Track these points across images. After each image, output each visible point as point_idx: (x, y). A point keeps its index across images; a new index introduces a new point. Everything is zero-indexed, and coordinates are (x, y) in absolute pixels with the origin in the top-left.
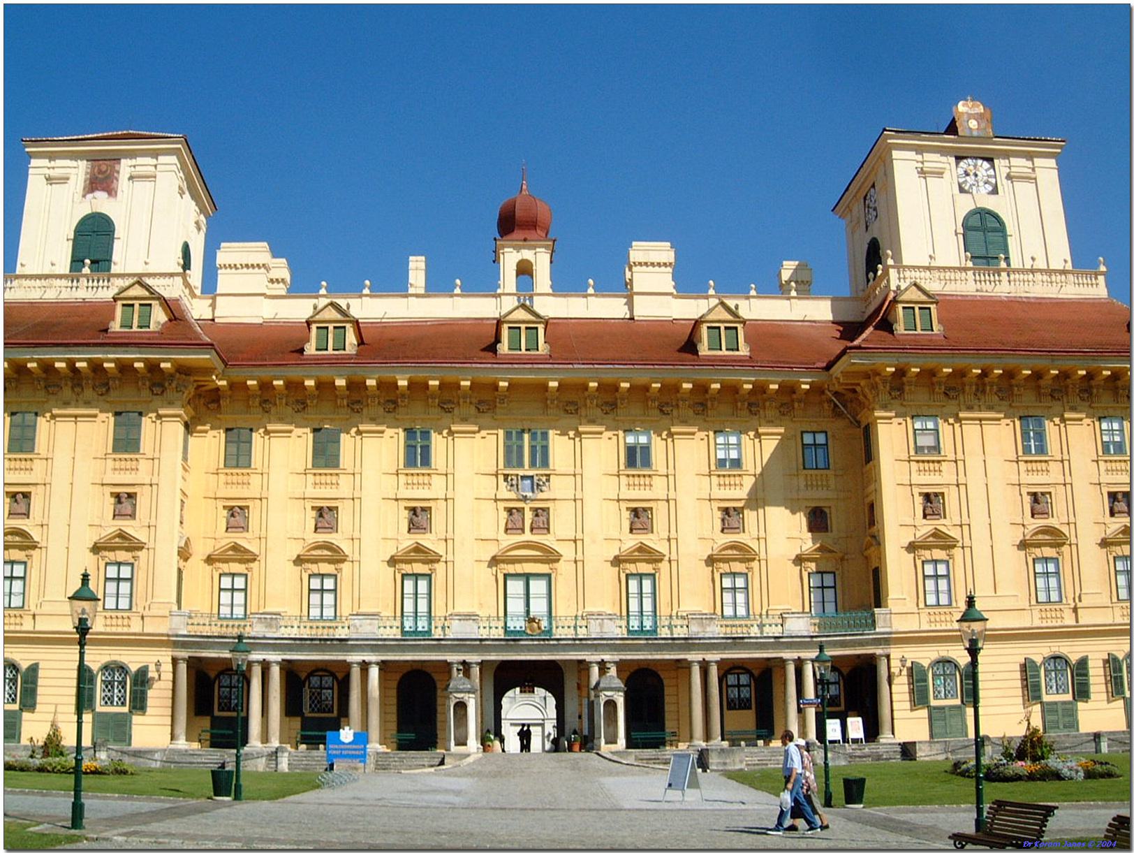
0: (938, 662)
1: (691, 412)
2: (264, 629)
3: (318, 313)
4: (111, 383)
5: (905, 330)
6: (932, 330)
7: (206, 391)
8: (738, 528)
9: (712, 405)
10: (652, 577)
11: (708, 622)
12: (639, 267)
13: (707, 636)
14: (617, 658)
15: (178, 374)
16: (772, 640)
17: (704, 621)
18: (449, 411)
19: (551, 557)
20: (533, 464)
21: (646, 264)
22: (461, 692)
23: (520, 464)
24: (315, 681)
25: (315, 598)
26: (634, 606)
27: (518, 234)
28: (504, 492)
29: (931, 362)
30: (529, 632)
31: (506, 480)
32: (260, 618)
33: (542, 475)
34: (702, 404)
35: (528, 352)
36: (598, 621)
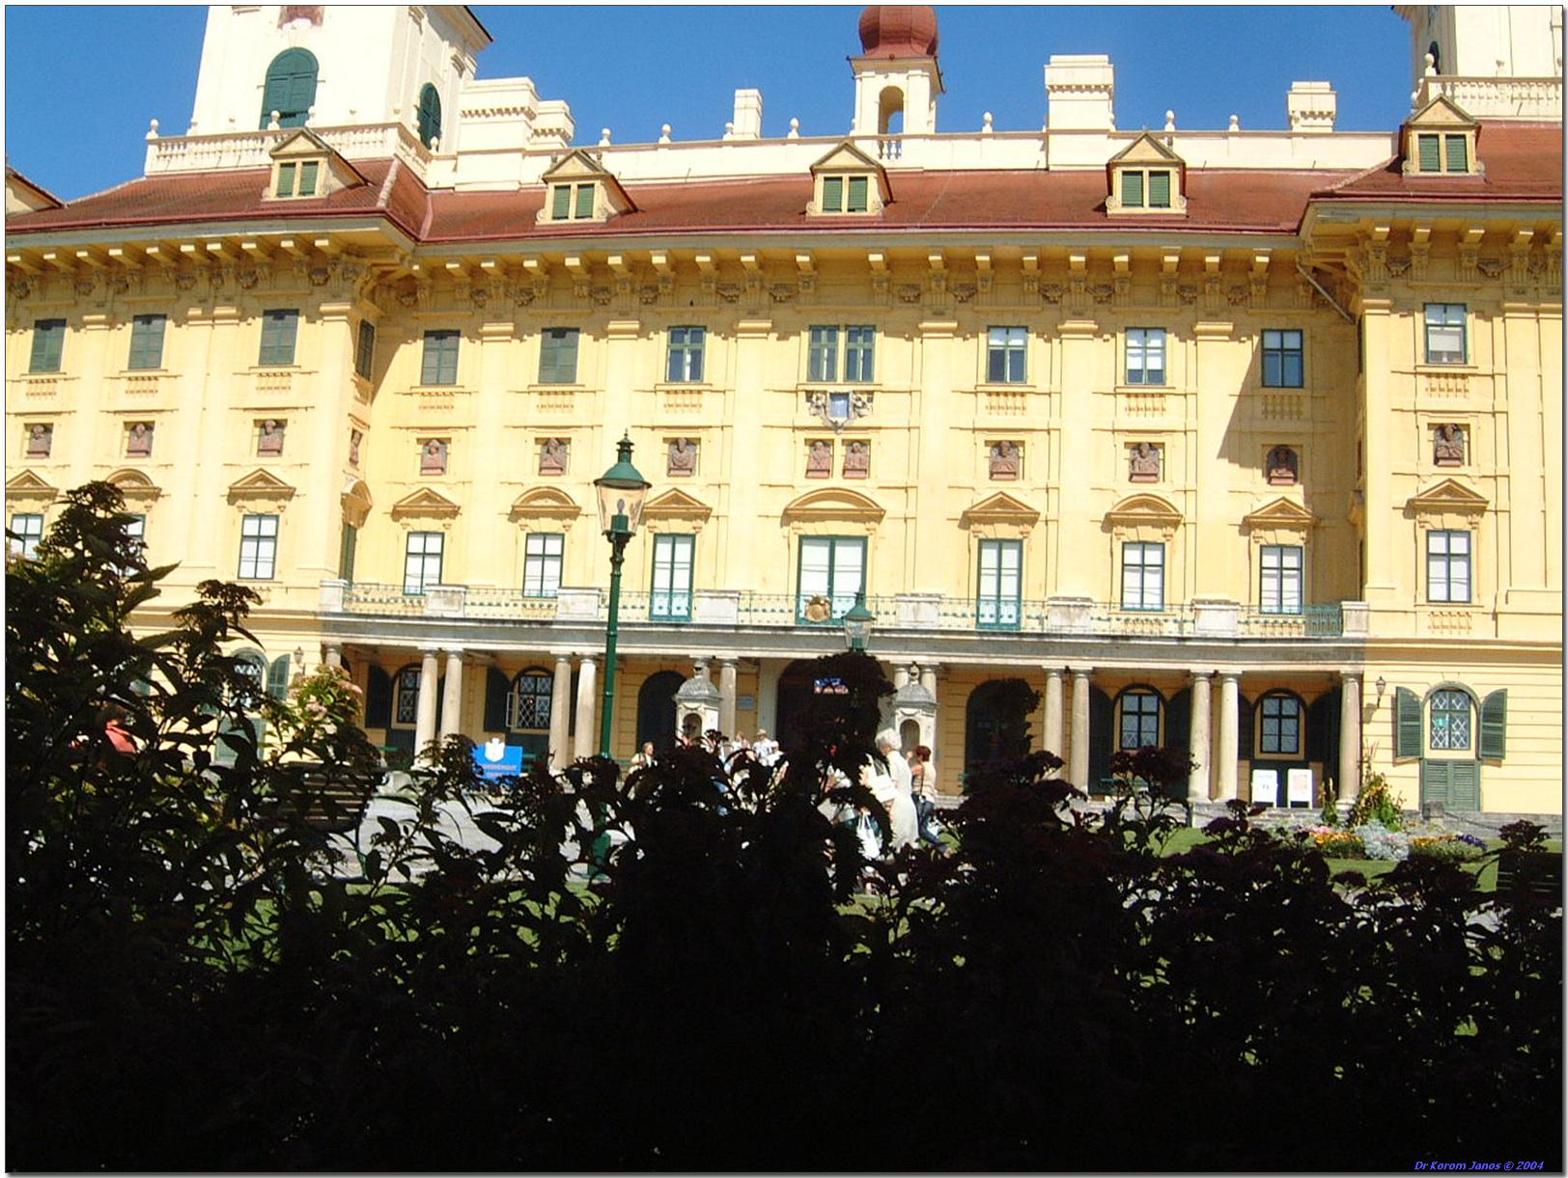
0: (1441, 690)
1: (1090, 299)
2: (443, 607)
3: (557, 168)
4: (258, 270)
5: (1421, 170)
6: (1467, 171)
7: (399, 280)
8: (1155, 475)
9: (1122, 289)
10: (1018, 545)
11: (1077, 610)
12: (1059, 93)
13: (1075, 631)
14: (936, 660)
15: (344, 257)
16: (1175, 643)
17: (1072, 609)
18: (732, 300)
19: (872, 514)
20: (850, 375)
21: (1069, 88)
22: (694, 700)
23: (831, 377)
24: (527, 683)
25: (534, 566)
26: (988, 587)
27: (884, 51)
28: (806, 415)
29: (1449, 220)
30: (810, 618)
31: (809, 399)
32: (438, 591)
33: (862, 392)
34: (1108, 287)
35: (851, 214)
36: (911, 605)
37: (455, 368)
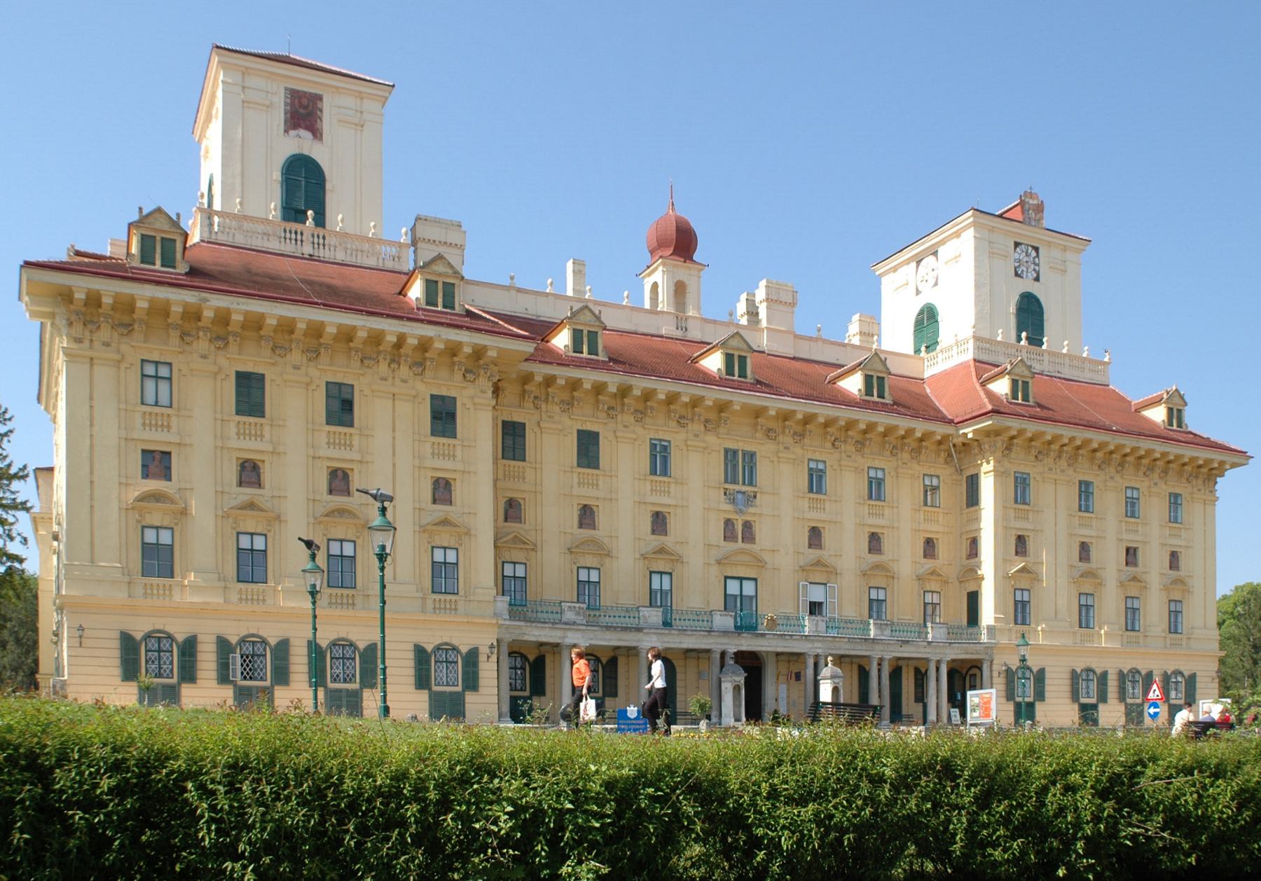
9: (870, 444)
19: (760, 563)
31: (725, 494)
35: (739, 379)
37: (524, 449)
